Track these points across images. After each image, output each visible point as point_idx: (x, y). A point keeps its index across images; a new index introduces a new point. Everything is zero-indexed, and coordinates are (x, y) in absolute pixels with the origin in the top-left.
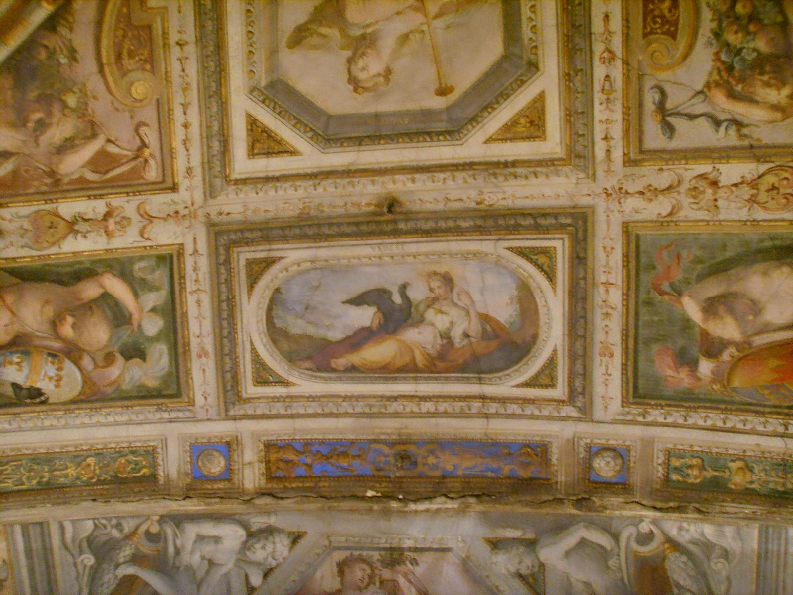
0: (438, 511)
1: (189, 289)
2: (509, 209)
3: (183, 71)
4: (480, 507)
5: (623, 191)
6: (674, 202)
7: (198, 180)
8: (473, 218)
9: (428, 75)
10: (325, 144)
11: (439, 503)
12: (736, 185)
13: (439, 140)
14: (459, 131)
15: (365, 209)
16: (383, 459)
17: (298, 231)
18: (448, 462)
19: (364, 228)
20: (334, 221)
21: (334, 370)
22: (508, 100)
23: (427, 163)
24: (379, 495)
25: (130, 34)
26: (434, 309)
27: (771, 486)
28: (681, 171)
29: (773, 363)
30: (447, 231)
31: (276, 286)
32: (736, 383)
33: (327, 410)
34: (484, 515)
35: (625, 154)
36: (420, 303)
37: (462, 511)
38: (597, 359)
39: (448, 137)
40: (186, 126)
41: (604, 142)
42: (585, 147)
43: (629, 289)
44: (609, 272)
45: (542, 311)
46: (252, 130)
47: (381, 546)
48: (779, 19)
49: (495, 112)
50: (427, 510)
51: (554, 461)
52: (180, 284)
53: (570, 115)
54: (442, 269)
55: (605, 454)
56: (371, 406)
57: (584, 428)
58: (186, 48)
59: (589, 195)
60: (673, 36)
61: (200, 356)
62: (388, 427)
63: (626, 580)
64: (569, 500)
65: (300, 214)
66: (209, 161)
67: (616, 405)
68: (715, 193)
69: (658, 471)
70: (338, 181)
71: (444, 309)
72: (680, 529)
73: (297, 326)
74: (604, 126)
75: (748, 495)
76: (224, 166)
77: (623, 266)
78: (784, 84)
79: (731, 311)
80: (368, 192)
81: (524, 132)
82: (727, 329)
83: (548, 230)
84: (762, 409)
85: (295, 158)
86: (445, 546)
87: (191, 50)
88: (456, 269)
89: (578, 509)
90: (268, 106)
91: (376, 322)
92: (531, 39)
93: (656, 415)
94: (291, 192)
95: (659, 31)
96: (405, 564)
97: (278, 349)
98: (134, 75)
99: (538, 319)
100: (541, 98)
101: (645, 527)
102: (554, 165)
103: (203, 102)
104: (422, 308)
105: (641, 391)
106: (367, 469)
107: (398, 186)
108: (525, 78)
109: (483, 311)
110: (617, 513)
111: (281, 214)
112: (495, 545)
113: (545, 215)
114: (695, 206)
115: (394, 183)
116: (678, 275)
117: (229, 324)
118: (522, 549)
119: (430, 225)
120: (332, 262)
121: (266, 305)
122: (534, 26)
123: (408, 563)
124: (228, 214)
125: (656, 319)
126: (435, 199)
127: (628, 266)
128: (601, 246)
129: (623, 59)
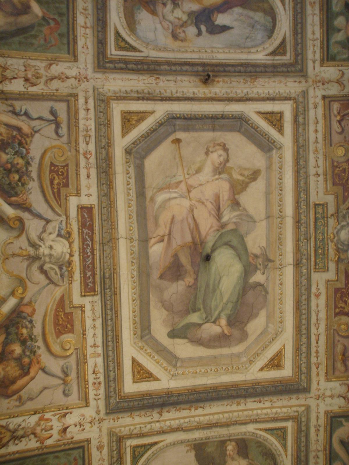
1: (319, 41)
2: (142, 74)
3: (317, 161)
5: (78, 79)
6: (49, 71)
7: (311, 101)
8: (161, 70)
9: (186, 151)
10: (242, 116)
12: (15, 78)
13: (180, 114)
14: (169, 119)
15: (220, 79)
17: (258, 70)
19: (221, 69)
20: (237, 74)
22: (141, 134)
23: (186, 102)
25: (344, 181)
26: (182, 21)
28: (45, 88)
30: (175, 64)
31: (270, 40)
35: (77, 100)
36: (190, 25)
39: (174, 115)
40: (316, 131)
42: (99, 106)
43: (73, 24)
44: (85, 34)
45: (122, 15)
46: (281, 126)
49: (149, 128)
52: (323, 45)
54: (178, 43)
58: (315, 173)
59: (97, 79)
60: (52, 164)
61: (314, 3)
66: (305, 111)
68: (26, 75)
70: (235, 96)
71: (177, 20)
73: (259, 16)
74: (89, 116)
76: (297, 108)
77: (77, 36)
80: (219, 88)
81: (133, 116)
83: (119, 60)
85: (258, 110)
87: (312, 171)
88: (170, 42)
90: (272, 139)
91: (215, 16)
92: (129, 167)
94: (260, 91)
95: (60, 167)
97: (270, 5)
98: (343, 159)
99: (124, 10)
100: (124, 135)
102: (117, 97)
103: (307, 143)
104: (189, 22)
107: (202, 91)
108: (133, 145)
109: (155, 17)
111: (267, 80)
113: (122, 69)
114: (37, 68)
115: (204, 93)
117: (297, 20)
119: (185, 68)
120: (239, 51)
121: (276, 29)
122: (128, 174)
124: (295, 82)
125: (57, 5)
126: (182, 82)
127: (74, 37)
128: (90, 50)
129: (79, 152)
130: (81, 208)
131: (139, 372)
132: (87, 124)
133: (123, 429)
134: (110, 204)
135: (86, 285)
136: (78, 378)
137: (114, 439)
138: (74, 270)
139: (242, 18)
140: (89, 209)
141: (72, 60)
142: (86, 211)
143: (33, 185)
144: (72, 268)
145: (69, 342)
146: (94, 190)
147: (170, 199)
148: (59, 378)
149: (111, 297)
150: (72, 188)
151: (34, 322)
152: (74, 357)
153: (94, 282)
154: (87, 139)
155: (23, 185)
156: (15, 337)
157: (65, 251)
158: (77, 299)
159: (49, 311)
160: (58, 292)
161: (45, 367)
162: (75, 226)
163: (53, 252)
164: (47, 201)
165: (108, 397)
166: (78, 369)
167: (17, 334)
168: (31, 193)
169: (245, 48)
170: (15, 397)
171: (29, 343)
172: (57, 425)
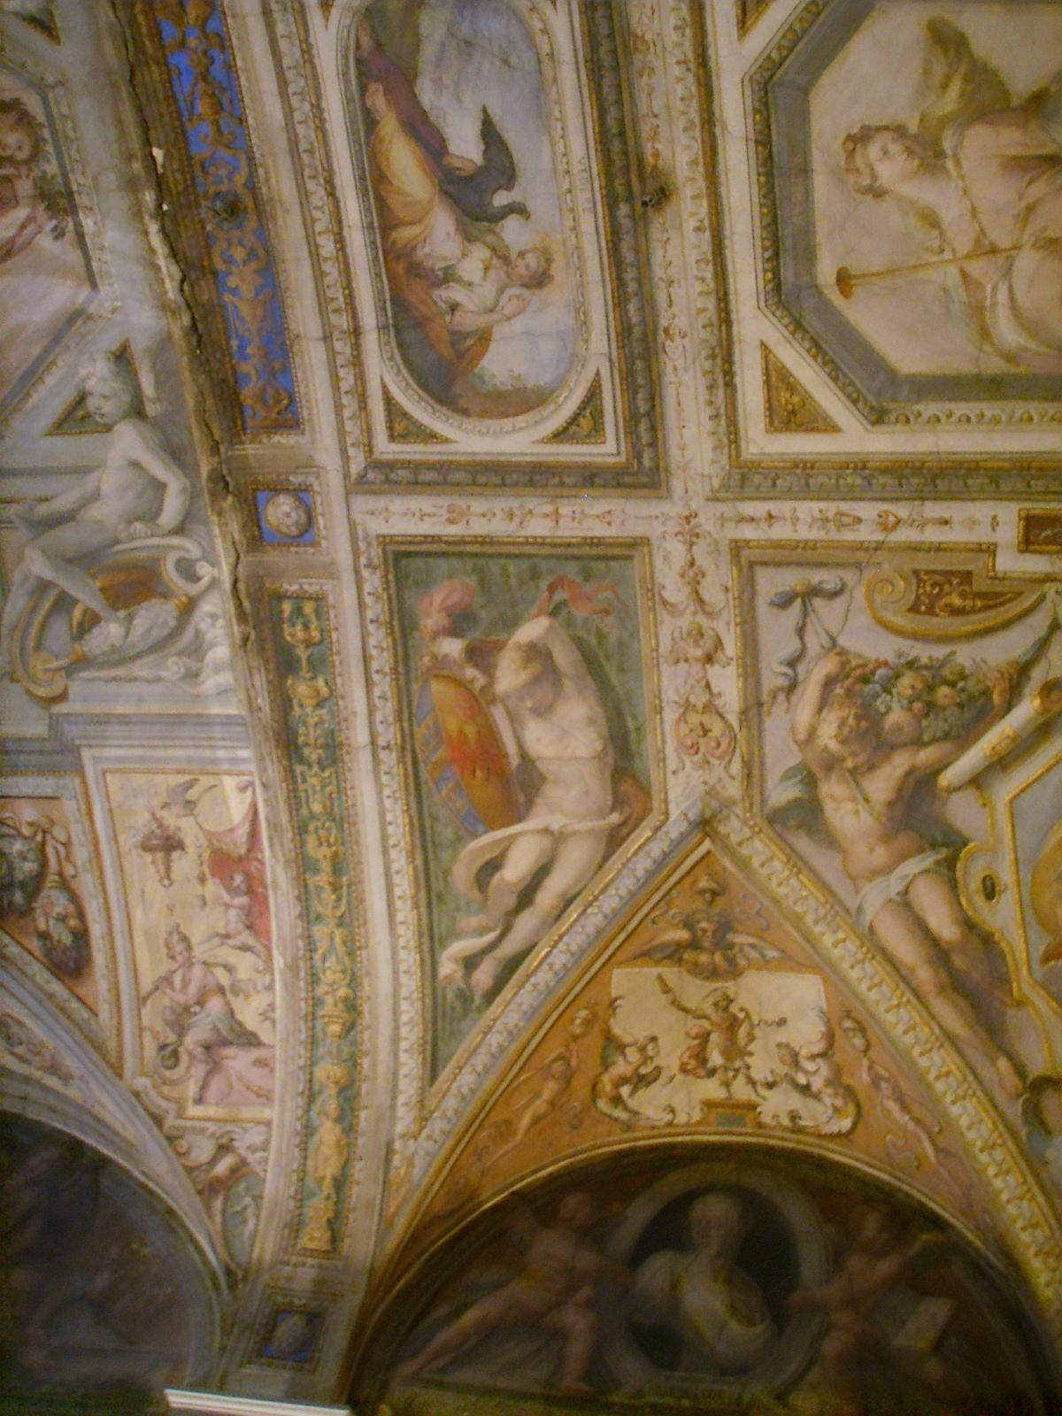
0: (156, 268)
2: (659, 376)
4: (177, 333)
5: (694, 539)
6: (681, 607)
8: (643, 321)
9: (870, 257)
10: (758, 83)
11: (170, 271)
12: (708, 686)
13: (765, 271)
14: (780, 304)
15: (648, 149)
16: (223, 172)
18: (241, 282)
19: (616, 147)
20: (626, 96)
21: (363, 90)
22: (828, 380)
23: (728, 252)
24: (160, 170)
26: (491, 258)
27: (302, 730)
28: (725, 616)
29: (471, 731)
30: (620, 282)
32: (437, 687)
33: (290, 75)
34: (166, 341)
36: (499, 237)
37: (165, 307)
38: (444, 502)
39: (770, 287)
41: (764, 514)
42: (758, 488)
43: (554, 545)
44: (574, 519)
45: (507, 423)
47: (71, 176)
48: (926, 737)
49: (810, 360)
50: (152, 251)
51: (276, 438)
53: (805, 468)
54: (557, 269)
55: (301, 511)
56: (310, 152)
57: (335, 482)
59: (686, 492)
60: (914, 609)
62: (281, 182)
63: (119, 547)
64: (220, 463)
65: (636, 36)
67: (377, 527)
68: (697, 660)
69: (290, 584)
71: (492, 273)
72: (214, 616)
74: (788, 515)
75: (283, 703)
77: (585, 538)
78: (844, 742)
79: (535, 680)
80: (677, 152)
81: (779, 401)
82: (509, 675)
83: (631, 433)
84: (406, 716)
86: (99, 281)
88: (558, 295)
89: (209, 477)
91: (457, 163)
92: (920, 415)
93: (373, 581)
94: (672, 20)
95: (921, 591)
96: (51, 218)
99: (491, 417)
100: (834, 429)
101: (204, 570)
102: (730, 442)
104: (490, 238)
105: (404, 562)
106: (200, 150)
107: (689, 206)
108: (861, 405)
109: (496, 334)
110: (216, 531)
112: (122, 358)
113: (653, 429)
114: (677, 634)
115: (695, 197)
116: (580, 613)
118: (126, 398)
119: (629, 256)
120: (554, 90)
122: (938, 420)
123: (54, 222)
125: (513, 581)
126: (670, 263)
128: (612, 507)
130: (1027, 544)
134: (1022, 469)
139: (447, 80)
141: (646, 550)
143: (965, 655)
146: (982, 510)
147: (1013, 306)
150: (976, 565)
154: (845, 520)
155: (963, 676)
164: (1006, 625)
168: (984, 662)
169: (540, 72)
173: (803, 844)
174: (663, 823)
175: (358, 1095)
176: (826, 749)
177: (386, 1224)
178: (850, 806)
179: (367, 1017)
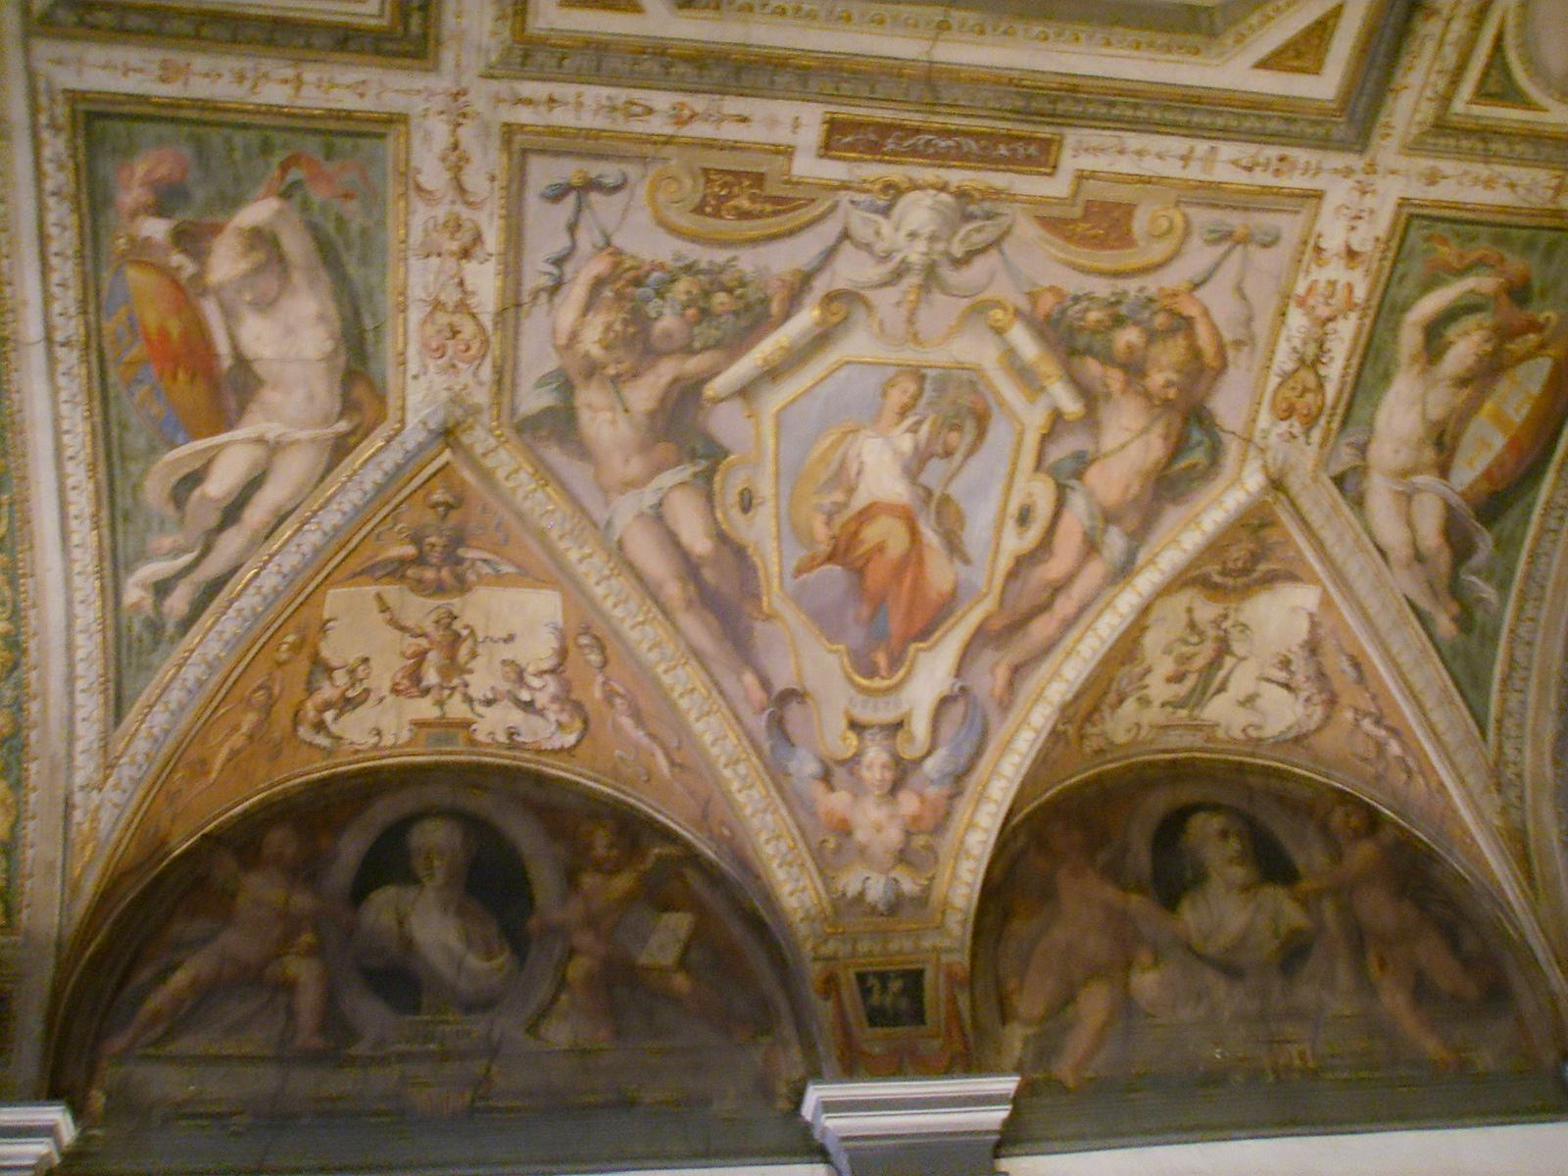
5: (460, 120)
12: (461, 283)
28: (488, 207)
29: (175, 328)
32: (132, 274)
35: (523, 126)
38: (156, 56)
41: (545, 97)
42: (542, 66)
43: (294, 116)
48: (697, 345)
53: (597, 49)
60: (699, 210)
67: (68, 79)
68: (452, 254)
74: (572, 100)
77: (331, 110)
78: (607, 348)
79: (257, 270)
82: (226, 262)
84: (91, 308)
93: (56, 146)
102: (515, 13)
105: (98, 125)
114: (431, 224)
116: (318, 195)
125: (238, 155)
127: (331, 117)
129: (672, 136)
130: (828, 149)
131: (1298, 55)
132: (594, 106)
133: (1418, 117)
134: (832, 69)
135: (1029, 160)
136: (1246, 209)
137: (1430, 140)
138: (981, 187)
140: (835, 128)
141: (402, 128)
142: (837, 137)
143: (747, 261)
144: (976, 189)
145: (1154, 220)
146: (784, 110)
148: (1226, 254)
149: (1078, 101)
151: (1080, 293)
152: (1192, 211)
153: (1029, 140)
155: (743, 284)
156: (1098, 337)
157: (928, 201)
158: (1057, 187)
159: (1061, 255)
160: (1027, 229)
161: (1190, 281)
162: (874, 171)
163: (927, 231)
165: (1324, 144)
166: (1226, 207)
167: (1094, 332)
170: (1231, 353)
171: (1123, 310)
172: (1335, 271)
173: (554, 454)
174: (398, 432)
175: (25, 745)
176: (587, 355)
177: (73, 888)
178: (608, 415)
179: (33, 656)
